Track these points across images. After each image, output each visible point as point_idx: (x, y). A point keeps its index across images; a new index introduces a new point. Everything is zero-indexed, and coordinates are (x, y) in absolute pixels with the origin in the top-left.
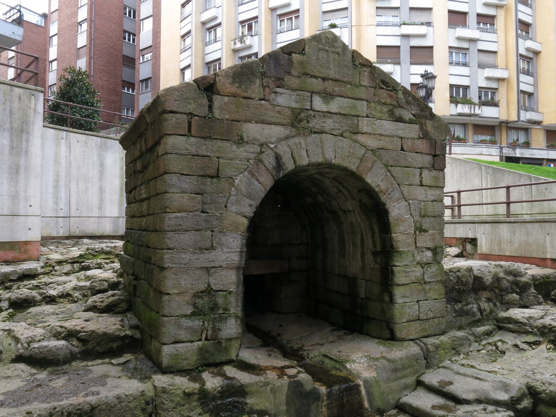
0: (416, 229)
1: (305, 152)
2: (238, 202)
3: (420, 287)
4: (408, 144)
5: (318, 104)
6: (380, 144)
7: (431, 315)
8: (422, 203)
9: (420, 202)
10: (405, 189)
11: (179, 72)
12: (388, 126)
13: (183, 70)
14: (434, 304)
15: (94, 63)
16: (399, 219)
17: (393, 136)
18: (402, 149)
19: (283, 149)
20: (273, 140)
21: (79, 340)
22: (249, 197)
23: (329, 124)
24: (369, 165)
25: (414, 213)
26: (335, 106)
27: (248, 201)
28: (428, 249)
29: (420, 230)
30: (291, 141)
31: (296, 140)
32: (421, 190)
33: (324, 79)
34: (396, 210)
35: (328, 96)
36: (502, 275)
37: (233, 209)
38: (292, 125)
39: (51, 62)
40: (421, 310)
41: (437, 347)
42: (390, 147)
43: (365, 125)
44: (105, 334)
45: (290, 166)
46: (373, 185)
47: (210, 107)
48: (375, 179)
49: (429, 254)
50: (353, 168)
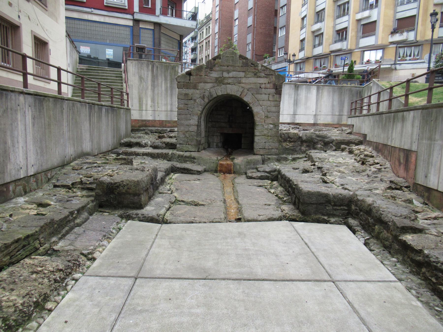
0: (265, 117)
1: (221, 91)
2: (198, 107)
3: (266, 137)
4: (263, 86)
5: (225, 75)
6: (249, 86)
7: (271, 148)
8: (269, 107)
9: (267, 107)
10: (261, 102)
11: (300, 20)
12: (254, 80)
13: (303, 19)
14: (273, 144)
15: (257, 18)
16: (258, 113)
17: (256, 83)
18: (260, 88)
19: (212, 90)
20: (209, 88)
21: (166, 144)
22: (201, 105)
23: (230, 81)
24: (245, 94)
25: (264, 111)
26: (231, 75)
27: (201, 107)
28: (271, 124)
29: (267, 117)
30: (215, 88)
31: (217, 87)
32: (269, 102)
33: (228, 66)
34: (256, 109)
35: (228, 72)
36: (314, 136)
37: (196, 109)
38: (216, 82)
39: (235, 20)
40: (266, 145)
41: (269, 159)
42: (254, 87)
43: (243, 80)
44: (171, 143)
45: (215, 95)
46: (246, 101)
47: (190, 80)
48: (247, 99)
49: (272, 126)
50: (238, 95)
